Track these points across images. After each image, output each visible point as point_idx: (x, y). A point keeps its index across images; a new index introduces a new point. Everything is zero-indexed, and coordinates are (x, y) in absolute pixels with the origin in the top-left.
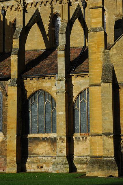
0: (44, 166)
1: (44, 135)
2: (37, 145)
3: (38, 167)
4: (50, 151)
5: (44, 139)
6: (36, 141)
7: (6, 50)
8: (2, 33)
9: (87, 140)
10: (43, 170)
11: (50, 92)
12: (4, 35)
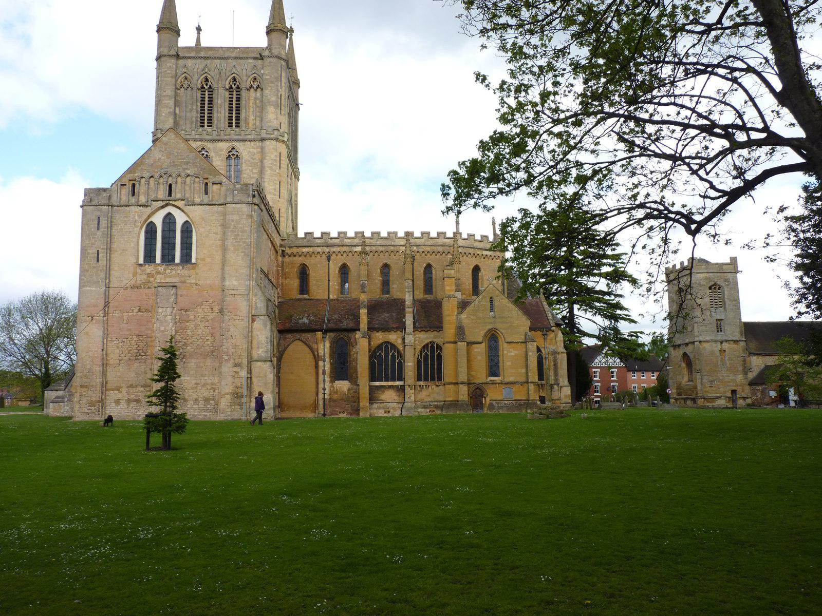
0: (391, 410)
1: (390, 383)
2: (384, 392)
3: (385, 412)
4: (395, 398)
5: (390, 387)
6: (382, 389)
7: (331, 296)
8: (327, 278)
9: (430, 388)
10: (390, 415)
11: (395, 344)
12: (329, 280)
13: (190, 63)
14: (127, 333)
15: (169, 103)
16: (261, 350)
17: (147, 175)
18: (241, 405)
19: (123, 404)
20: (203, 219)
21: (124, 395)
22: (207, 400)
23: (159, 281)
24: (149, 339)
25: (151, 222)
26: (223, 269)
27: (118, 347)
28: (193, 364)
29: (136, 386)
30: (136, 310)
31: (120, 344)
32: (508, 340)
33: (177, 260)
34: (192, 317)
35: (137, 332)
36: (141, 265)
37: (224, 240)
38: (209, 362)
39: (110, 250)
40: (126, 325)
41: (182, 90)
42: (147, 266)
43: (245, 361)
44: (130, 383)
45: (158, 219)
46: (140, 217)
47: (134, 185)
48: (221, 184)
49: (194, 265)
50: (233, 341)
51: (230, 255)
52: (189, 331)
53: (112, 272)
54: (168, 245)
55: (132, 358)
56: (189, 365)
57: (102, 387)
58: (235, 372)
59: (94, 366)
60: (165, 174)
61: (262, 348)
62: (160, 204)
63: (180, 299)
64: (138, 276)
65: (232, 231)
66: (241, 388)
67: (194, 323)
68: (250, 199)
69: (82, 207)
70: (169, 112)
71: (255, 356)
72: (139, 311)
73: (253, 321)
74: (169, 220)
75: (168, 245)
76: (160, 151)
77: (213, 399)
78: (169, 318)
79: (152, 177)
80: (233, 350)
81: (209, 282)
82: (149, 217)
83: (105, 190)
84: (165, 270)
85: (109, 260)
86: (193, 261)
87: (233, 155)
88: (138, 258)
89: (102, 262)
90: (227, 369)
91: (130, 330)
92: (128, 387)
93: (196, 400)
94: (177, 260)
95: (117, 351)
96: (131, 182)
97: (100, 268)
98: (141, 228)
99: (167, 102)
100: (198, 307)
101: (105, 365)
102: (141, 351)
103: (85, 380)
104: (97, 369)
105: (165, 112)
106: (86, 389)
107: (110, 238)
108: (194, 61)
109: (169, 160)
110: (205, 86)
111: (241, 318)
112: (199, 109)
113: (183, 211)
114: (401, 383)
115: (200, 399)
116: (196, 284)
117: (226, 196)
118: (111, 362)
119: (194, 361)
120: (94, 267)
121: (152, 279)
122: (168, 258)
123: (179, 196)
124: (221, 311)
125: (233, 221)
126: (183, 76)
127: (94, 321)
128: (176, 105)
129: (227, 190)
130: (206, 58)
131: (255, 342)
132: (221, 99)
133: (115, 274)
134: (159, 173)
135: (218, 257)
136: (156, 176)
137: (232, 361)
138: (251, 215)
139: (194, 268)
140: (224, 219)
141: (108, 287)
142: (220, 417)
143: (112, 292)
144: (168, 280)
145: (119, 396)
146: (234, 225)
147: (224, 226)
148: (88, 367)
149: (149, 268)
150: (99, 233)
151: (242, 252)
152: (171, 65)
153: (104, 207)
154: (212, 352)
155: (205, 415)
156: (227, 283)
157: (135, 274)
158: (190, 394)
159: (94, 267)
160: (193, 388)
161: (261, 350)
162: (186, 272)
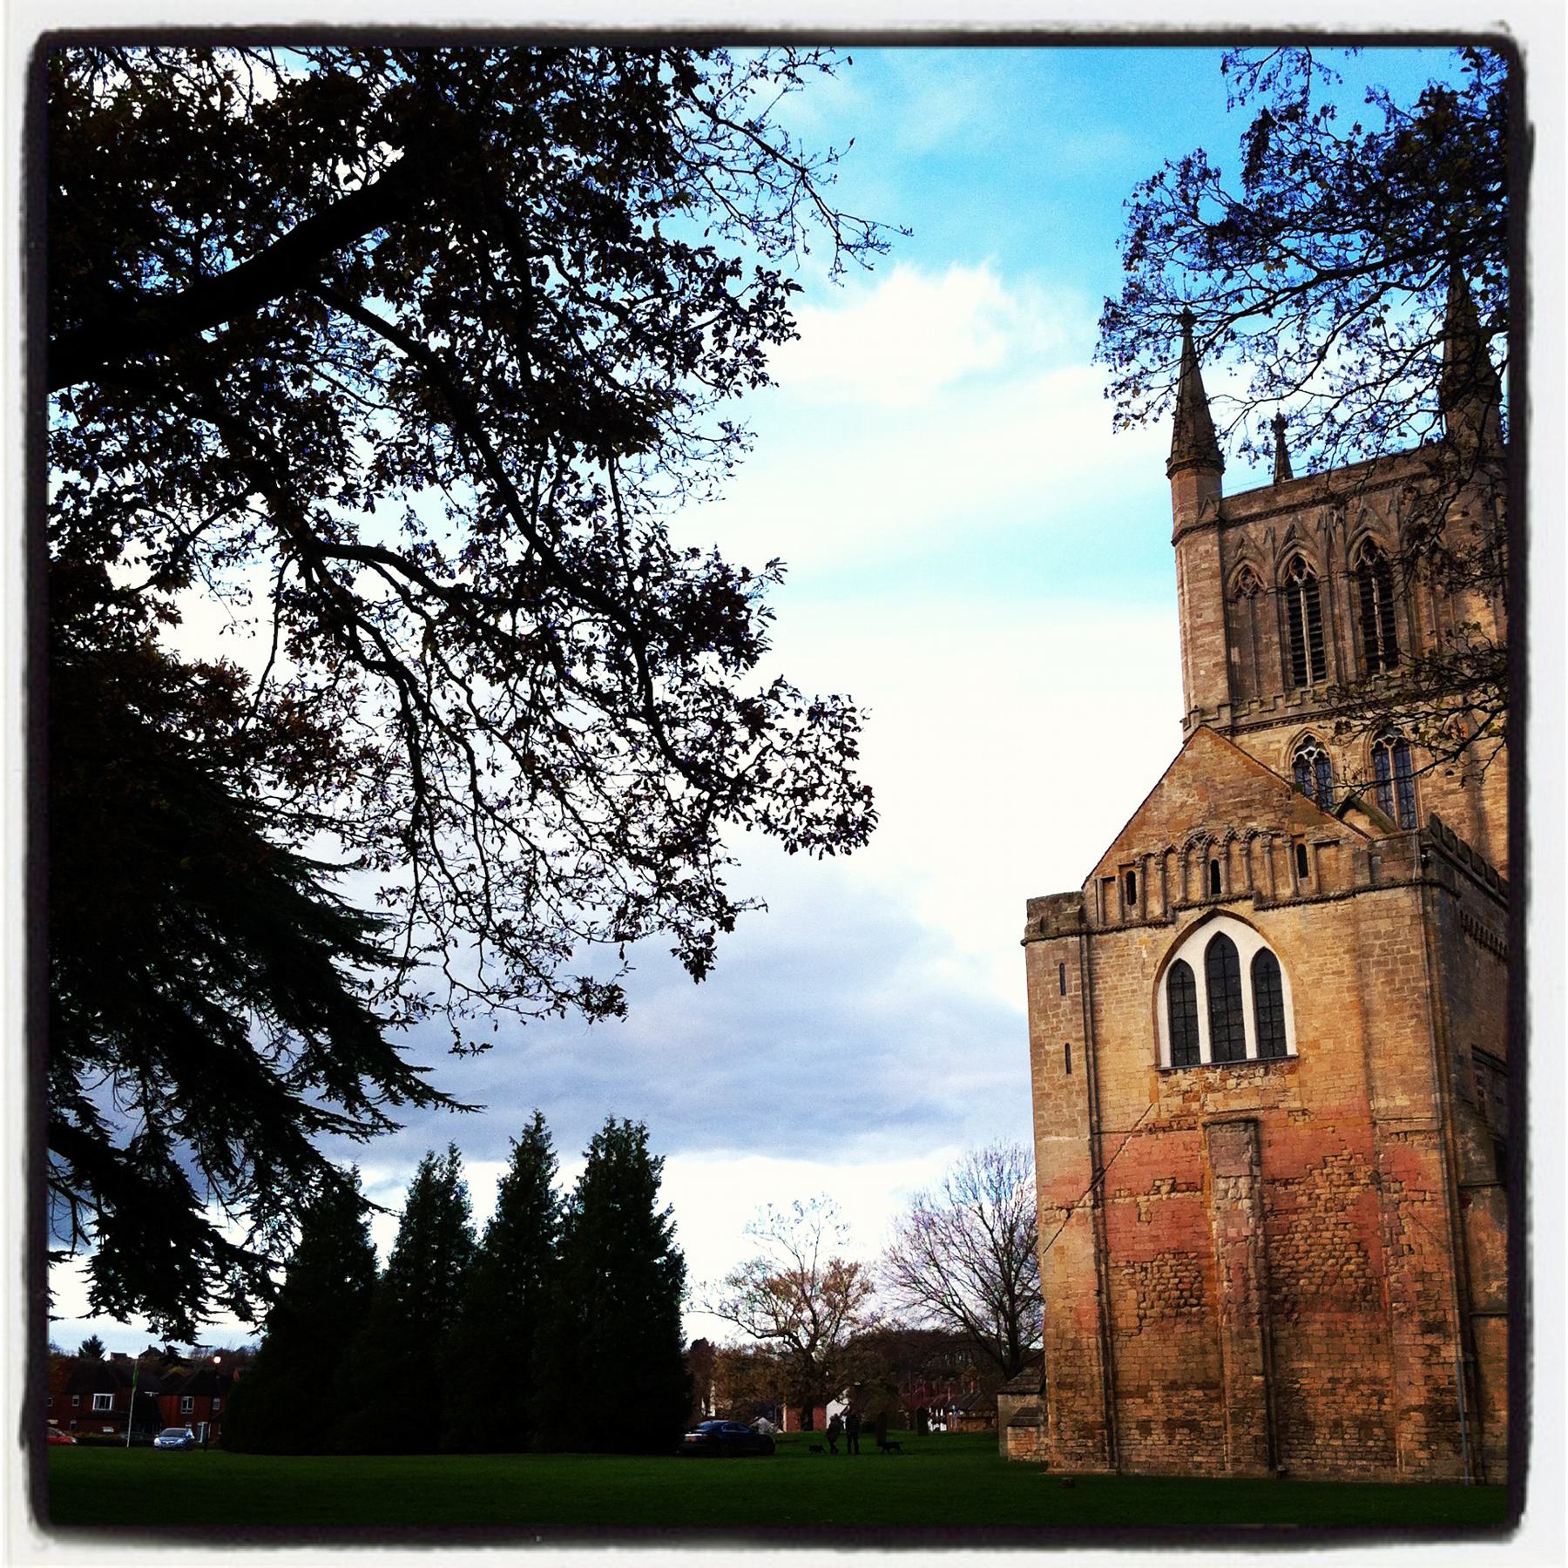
13: (1255, 531)
14: (1151, 1246)
15: (1213, 642)
16: (1495, 1285)
17: (1157, 848)
18: (1454, 1440)
19: (1158, 1436)
20: (1301, 938)
22: (1364, 1425)
23: (1211, 1109)
24: (1204, 1262)
25: (1180, 961)
26: (1367, 1065)
27: (1133, 1285)
28: (1318, 1326)
29: (1185, 1387)
30: (1165, 1189)
31: (1138, 1276)
33: (1251, 1052)
34: (1305, 1198)
35: (1174, 1244)
36: (1166, 1073)
37: (1361, 987)
38: (1358, 1321)
39: (1092, 1040)
40: (1145, 1228)
41: (1243, 601)
42: (1180, 1072)
43: (1453, 1317)
44: (1170, 1377)
45: (1194, 954)
46: (1152, 952)
47: (1131, 877)
48: (1336, 843)
49: (1294, 1062)
50: (1414, 1259)
51: (1381, 1027)
52: (1298, 1236)
53: (1103, 1094)
54: (1226, 1014)
55: (1167, 1311)
56: (1310, 1329)
57: (1107, 1387)
58: (1434, 1349)
59: (1085, 1334)
60: (1199, 839)
61: (1497, 1279)
62: (1194, 915)
63: (1268, 1152)
64: (1163, 1101)
65: (1378, 963)
66: (1452, 1392)
67: (1309, 1216)
68: (1416, 873)
69: (1023, 944)
70: (1215, 665)
71: (1481, 1300)
72: (1173, 1189)
73: (1464, 1203)
74: (1221, 950)
75: (1226, 1014)
76: (1183, 786)
77: (1381, 1424)
78: (1246, 1203)
79: (1171, 850)
80: (1419, 1287)
81: (1335, 1103)
82: (1174, 948)
83: (1069, 897)
84: (1224, 1080)
85: (1094, 1065)
86: (1291, 1050)
87: (1389, 741)
88: (1158, 1056)
89: (1080, 1072)
90: (1408, 1337)
92: (1165, 1388)
93: (1337, 1424)
94: (1251, 1052)
95: (1132, 1294)
96: (1125, 873)
97: (1077, 1088)
98: (1158, 979)
99: (1207, 640)
100: (1316, 1172)
101: (1107, 1328)
102: (1186, 1294)
103: (1066, 1370)
104: (1091, 1340)
105: (1207, 662)
106: (1070, 1394)
107: (1091, 1011)
108: (1261, 525)
109: (1205, 804)
110: (1296, 578)
111: (1428, 1196)
112: (1288, 639)
113: (1251, 925)
115: (1346, 1423)
116: (1304, 1112)
117: (1354, 871)
118: (1121, 1323)
120: (1062, 1087)
121: (1195, 1106)
122: (1228, 1050)
123: (1239, 888)
124: (1376, 1178)
125: (1377, 936)
126: (1240, 567)
127: (1073, 1220)
128: (1229, 644)
129: (1355, 856)
130: (1291, 509)
131: (1477, 1262)
132: (1342, 606)
133: (1112, 1096)
134: (1185, 839)
135: (1351, 1036)
136: (1180, 846)
137: (1417, 1318)
138: (1425, 913)
139: (1292, 1071)
140: (1356, 935)
141: (1097, 1132)
142: (1404, 1473)
143: (1109, 1144)
144: (1235, 1105)
145: (1147, 1412)
146: (1381, 946)
147: (1359, 953)
148: (1071, 1336)
149: (1185, 1080)
150: (1066, 1002)
151: (1411, 1017)
152: (1209, 547)
153: (1070, 939)
154: (1365, 1292)
155: (1363, 1468)
156: (1381, 1103)
157: (1155, 1096)
158: (1321, 1408)
159: (1062, 1087)
160: (1324, 1393)
161: (1495, 1285)
162: (1274, 1080)
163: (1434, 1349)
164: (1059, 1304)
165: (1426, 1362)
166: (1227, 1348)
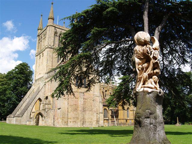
19: (72, 122)
21: (72, 120)
22: (90, 122)
32: (131, 110)
38: (91, 112)
90: (95, 114)
91: (73, 103)
104: (66, 113)
114: (108, 118)
119: (88, 112)
144: (82, 91)
163: (97, 115)
164: (63, 109)
165: (97, 117)
166: (80, 114)
